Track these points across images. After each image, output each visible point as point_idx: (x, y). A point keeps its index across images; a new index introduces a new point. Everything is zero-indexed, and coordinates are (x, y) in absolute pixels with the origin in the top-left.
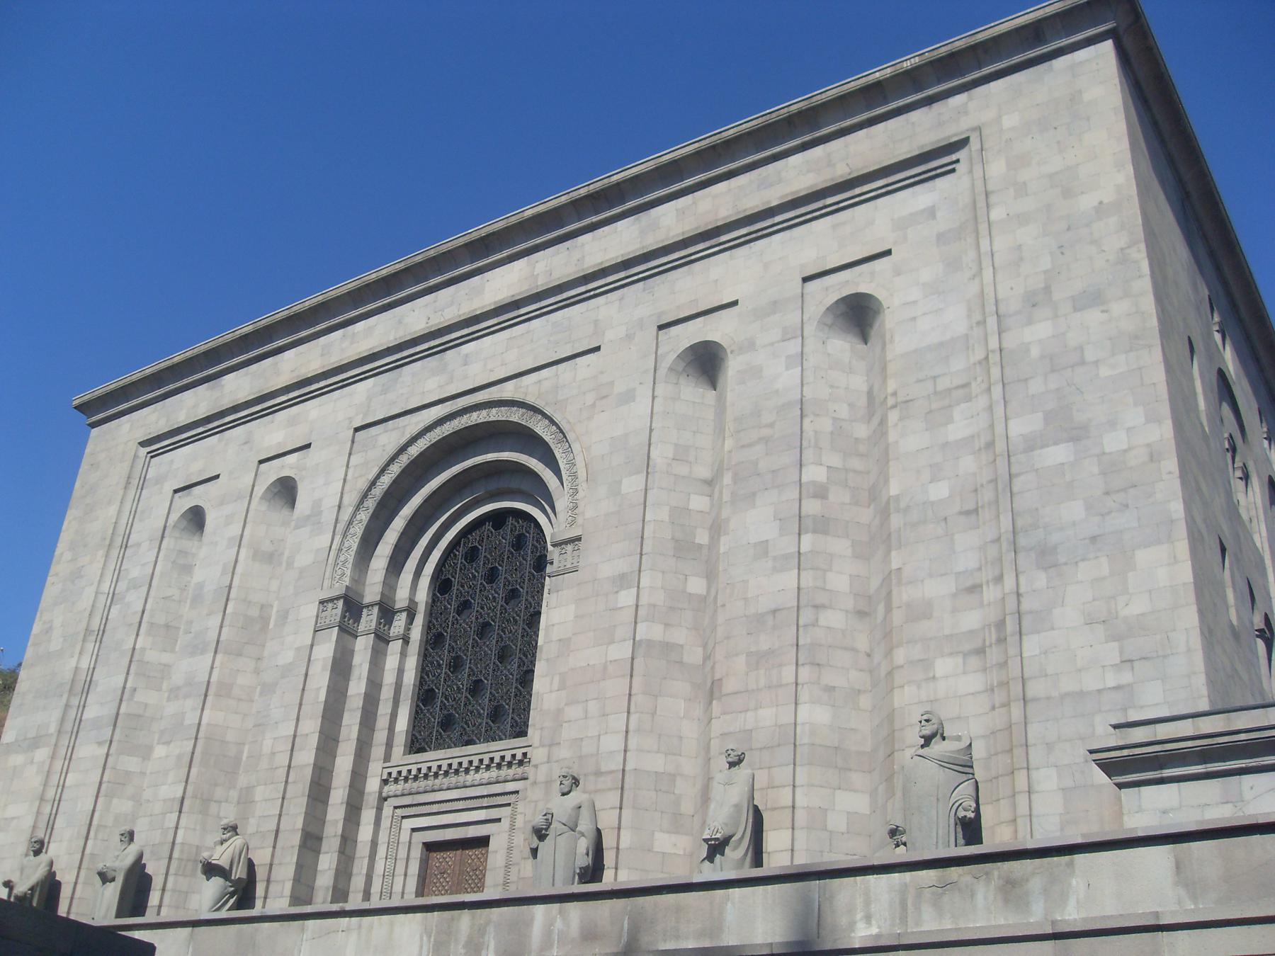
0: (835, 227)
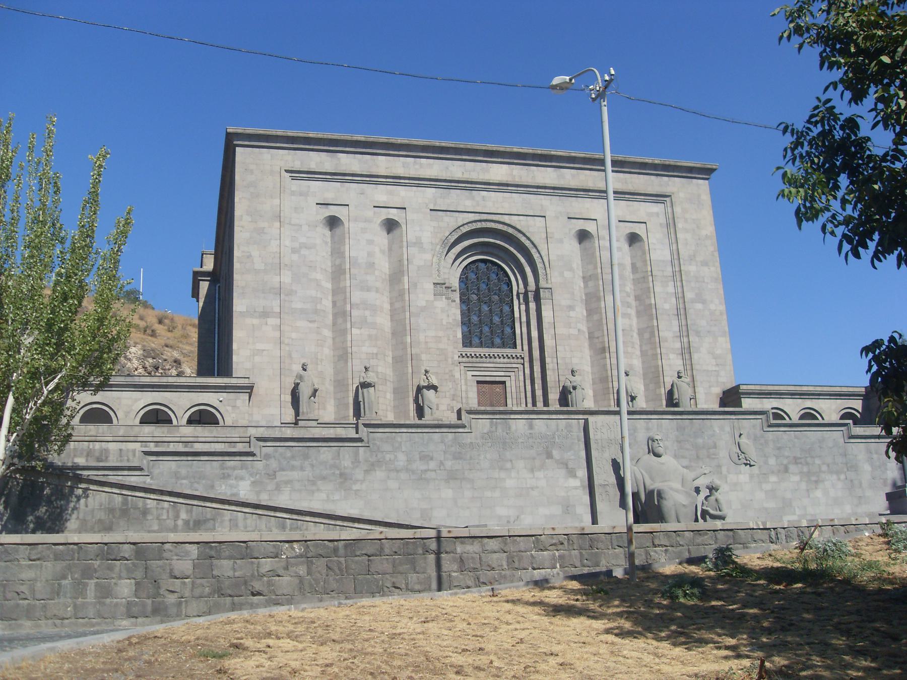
0: (628, 206)
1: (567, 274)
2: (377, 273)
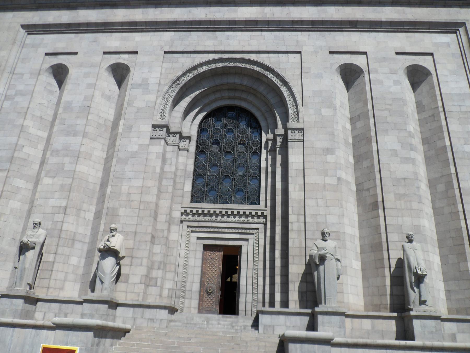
1: (325, 112)
2: (90, 118)
